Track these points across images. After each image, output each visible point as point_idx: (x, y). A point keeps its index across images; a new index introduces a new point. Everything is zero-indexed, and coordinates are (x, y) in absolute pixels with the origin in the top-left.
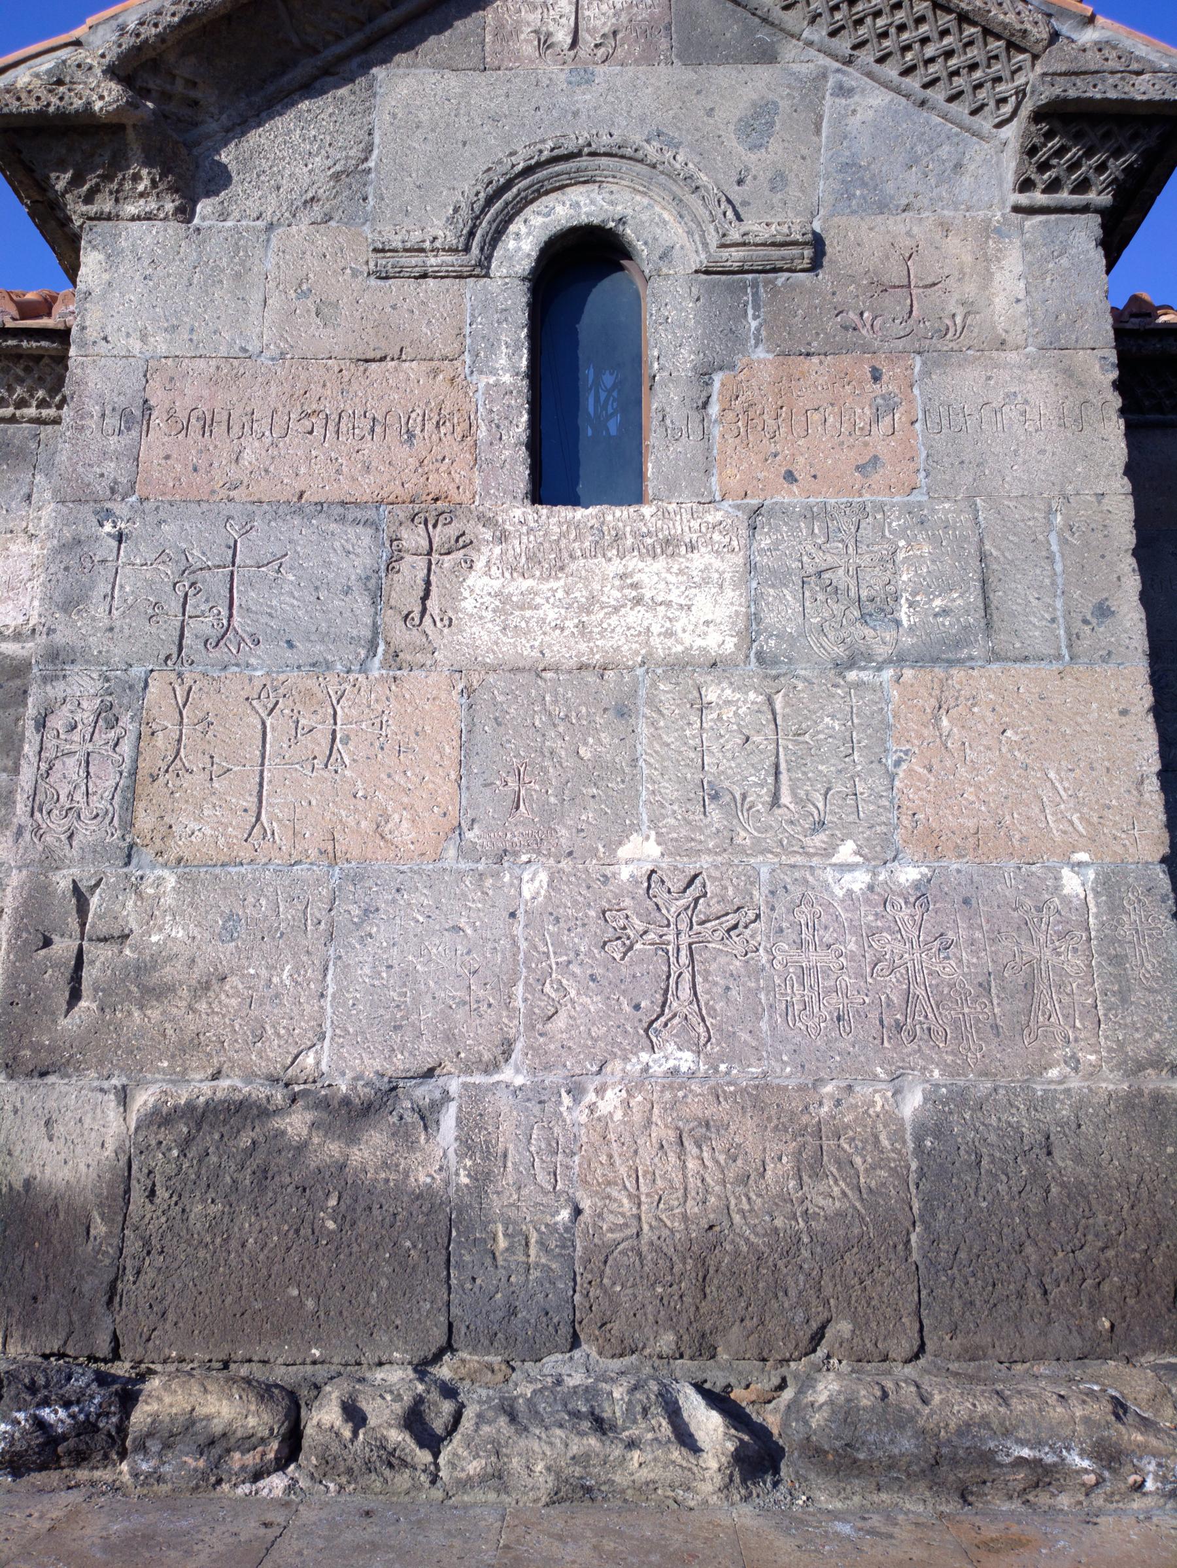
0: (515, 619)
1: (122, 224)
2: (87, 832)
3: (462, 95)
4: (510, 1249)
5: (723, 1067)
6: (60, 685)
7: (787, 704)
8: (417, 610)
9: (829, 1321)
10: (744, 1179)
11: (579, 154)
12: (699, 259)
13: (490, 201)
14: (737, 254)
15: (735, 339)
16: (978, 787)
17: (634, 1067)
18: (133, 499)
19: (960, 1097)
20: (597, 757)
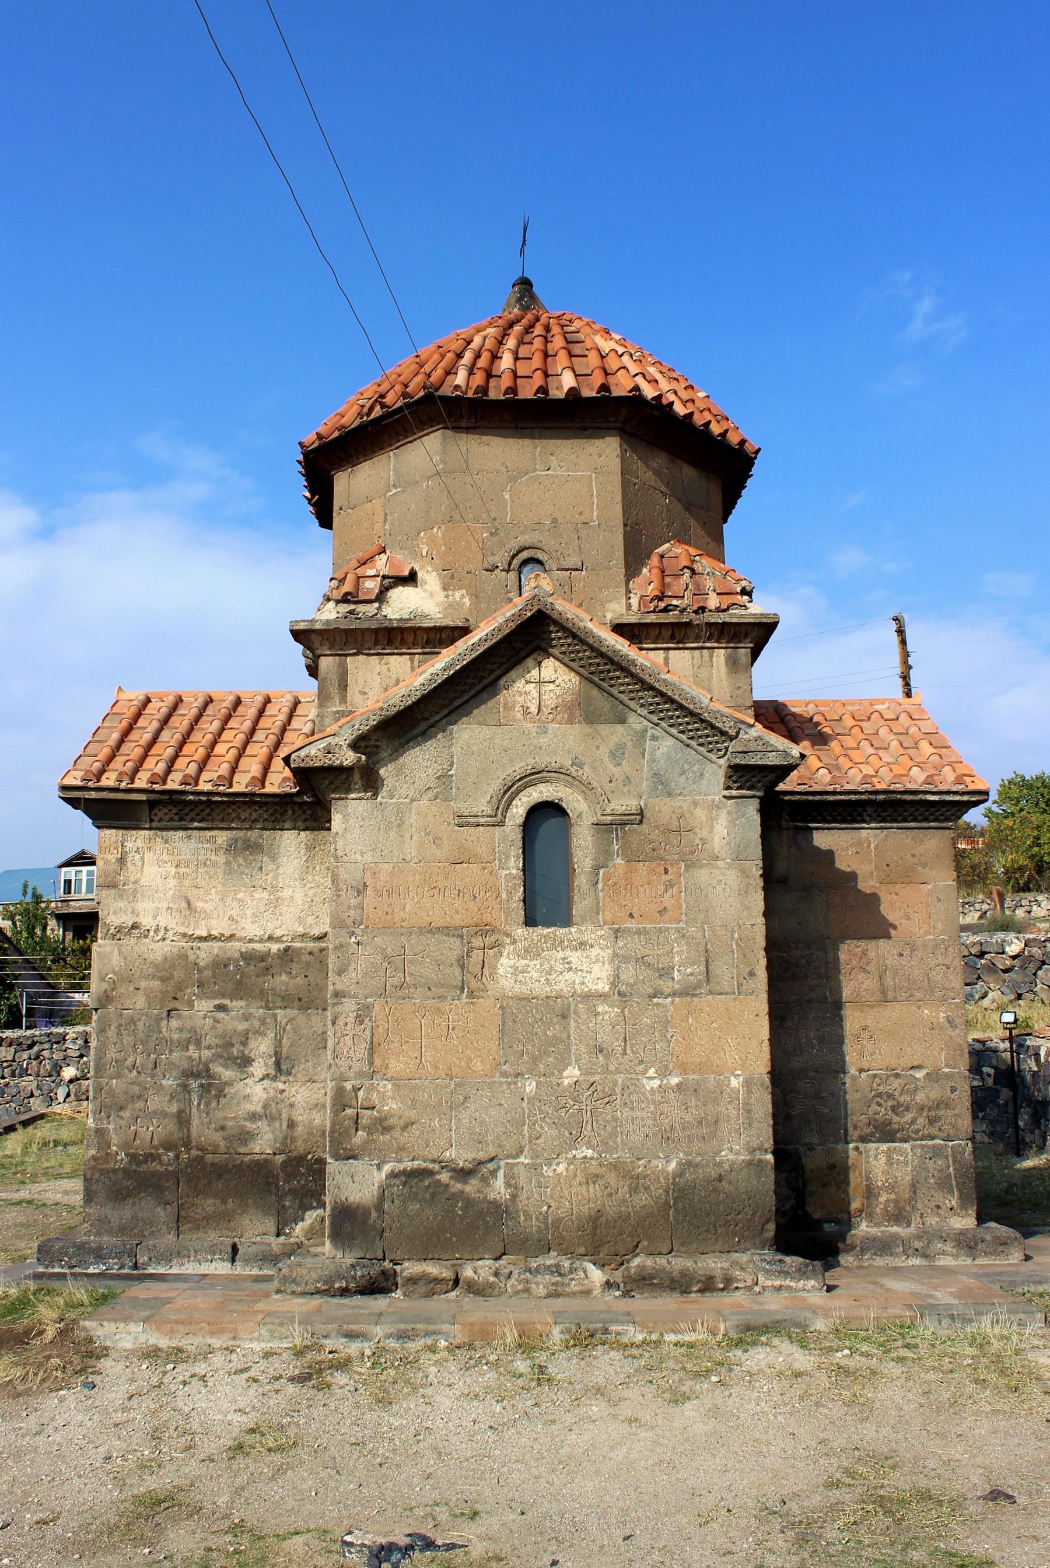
0: (520, 977)
1: (348, 801)
2: (356, 1067)
3: (491, 739)
4: (525, 1220)
5: (603, 1155)
6: (340, 1007)
7: (630, 1013)
8: (480, 973)
9: (639, 1242)
10: (610, 1195)
11: (543, 771)
12: (595, 820)
13: (505, 793)
14: (609, 818)
15: (608, 855)
16: (702, 1046)
17: (570, 1156)
18: (362, 927)
19: (689, 1164)
20: (554, 1036)
